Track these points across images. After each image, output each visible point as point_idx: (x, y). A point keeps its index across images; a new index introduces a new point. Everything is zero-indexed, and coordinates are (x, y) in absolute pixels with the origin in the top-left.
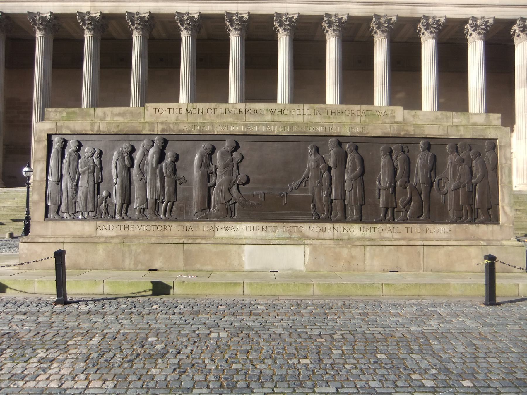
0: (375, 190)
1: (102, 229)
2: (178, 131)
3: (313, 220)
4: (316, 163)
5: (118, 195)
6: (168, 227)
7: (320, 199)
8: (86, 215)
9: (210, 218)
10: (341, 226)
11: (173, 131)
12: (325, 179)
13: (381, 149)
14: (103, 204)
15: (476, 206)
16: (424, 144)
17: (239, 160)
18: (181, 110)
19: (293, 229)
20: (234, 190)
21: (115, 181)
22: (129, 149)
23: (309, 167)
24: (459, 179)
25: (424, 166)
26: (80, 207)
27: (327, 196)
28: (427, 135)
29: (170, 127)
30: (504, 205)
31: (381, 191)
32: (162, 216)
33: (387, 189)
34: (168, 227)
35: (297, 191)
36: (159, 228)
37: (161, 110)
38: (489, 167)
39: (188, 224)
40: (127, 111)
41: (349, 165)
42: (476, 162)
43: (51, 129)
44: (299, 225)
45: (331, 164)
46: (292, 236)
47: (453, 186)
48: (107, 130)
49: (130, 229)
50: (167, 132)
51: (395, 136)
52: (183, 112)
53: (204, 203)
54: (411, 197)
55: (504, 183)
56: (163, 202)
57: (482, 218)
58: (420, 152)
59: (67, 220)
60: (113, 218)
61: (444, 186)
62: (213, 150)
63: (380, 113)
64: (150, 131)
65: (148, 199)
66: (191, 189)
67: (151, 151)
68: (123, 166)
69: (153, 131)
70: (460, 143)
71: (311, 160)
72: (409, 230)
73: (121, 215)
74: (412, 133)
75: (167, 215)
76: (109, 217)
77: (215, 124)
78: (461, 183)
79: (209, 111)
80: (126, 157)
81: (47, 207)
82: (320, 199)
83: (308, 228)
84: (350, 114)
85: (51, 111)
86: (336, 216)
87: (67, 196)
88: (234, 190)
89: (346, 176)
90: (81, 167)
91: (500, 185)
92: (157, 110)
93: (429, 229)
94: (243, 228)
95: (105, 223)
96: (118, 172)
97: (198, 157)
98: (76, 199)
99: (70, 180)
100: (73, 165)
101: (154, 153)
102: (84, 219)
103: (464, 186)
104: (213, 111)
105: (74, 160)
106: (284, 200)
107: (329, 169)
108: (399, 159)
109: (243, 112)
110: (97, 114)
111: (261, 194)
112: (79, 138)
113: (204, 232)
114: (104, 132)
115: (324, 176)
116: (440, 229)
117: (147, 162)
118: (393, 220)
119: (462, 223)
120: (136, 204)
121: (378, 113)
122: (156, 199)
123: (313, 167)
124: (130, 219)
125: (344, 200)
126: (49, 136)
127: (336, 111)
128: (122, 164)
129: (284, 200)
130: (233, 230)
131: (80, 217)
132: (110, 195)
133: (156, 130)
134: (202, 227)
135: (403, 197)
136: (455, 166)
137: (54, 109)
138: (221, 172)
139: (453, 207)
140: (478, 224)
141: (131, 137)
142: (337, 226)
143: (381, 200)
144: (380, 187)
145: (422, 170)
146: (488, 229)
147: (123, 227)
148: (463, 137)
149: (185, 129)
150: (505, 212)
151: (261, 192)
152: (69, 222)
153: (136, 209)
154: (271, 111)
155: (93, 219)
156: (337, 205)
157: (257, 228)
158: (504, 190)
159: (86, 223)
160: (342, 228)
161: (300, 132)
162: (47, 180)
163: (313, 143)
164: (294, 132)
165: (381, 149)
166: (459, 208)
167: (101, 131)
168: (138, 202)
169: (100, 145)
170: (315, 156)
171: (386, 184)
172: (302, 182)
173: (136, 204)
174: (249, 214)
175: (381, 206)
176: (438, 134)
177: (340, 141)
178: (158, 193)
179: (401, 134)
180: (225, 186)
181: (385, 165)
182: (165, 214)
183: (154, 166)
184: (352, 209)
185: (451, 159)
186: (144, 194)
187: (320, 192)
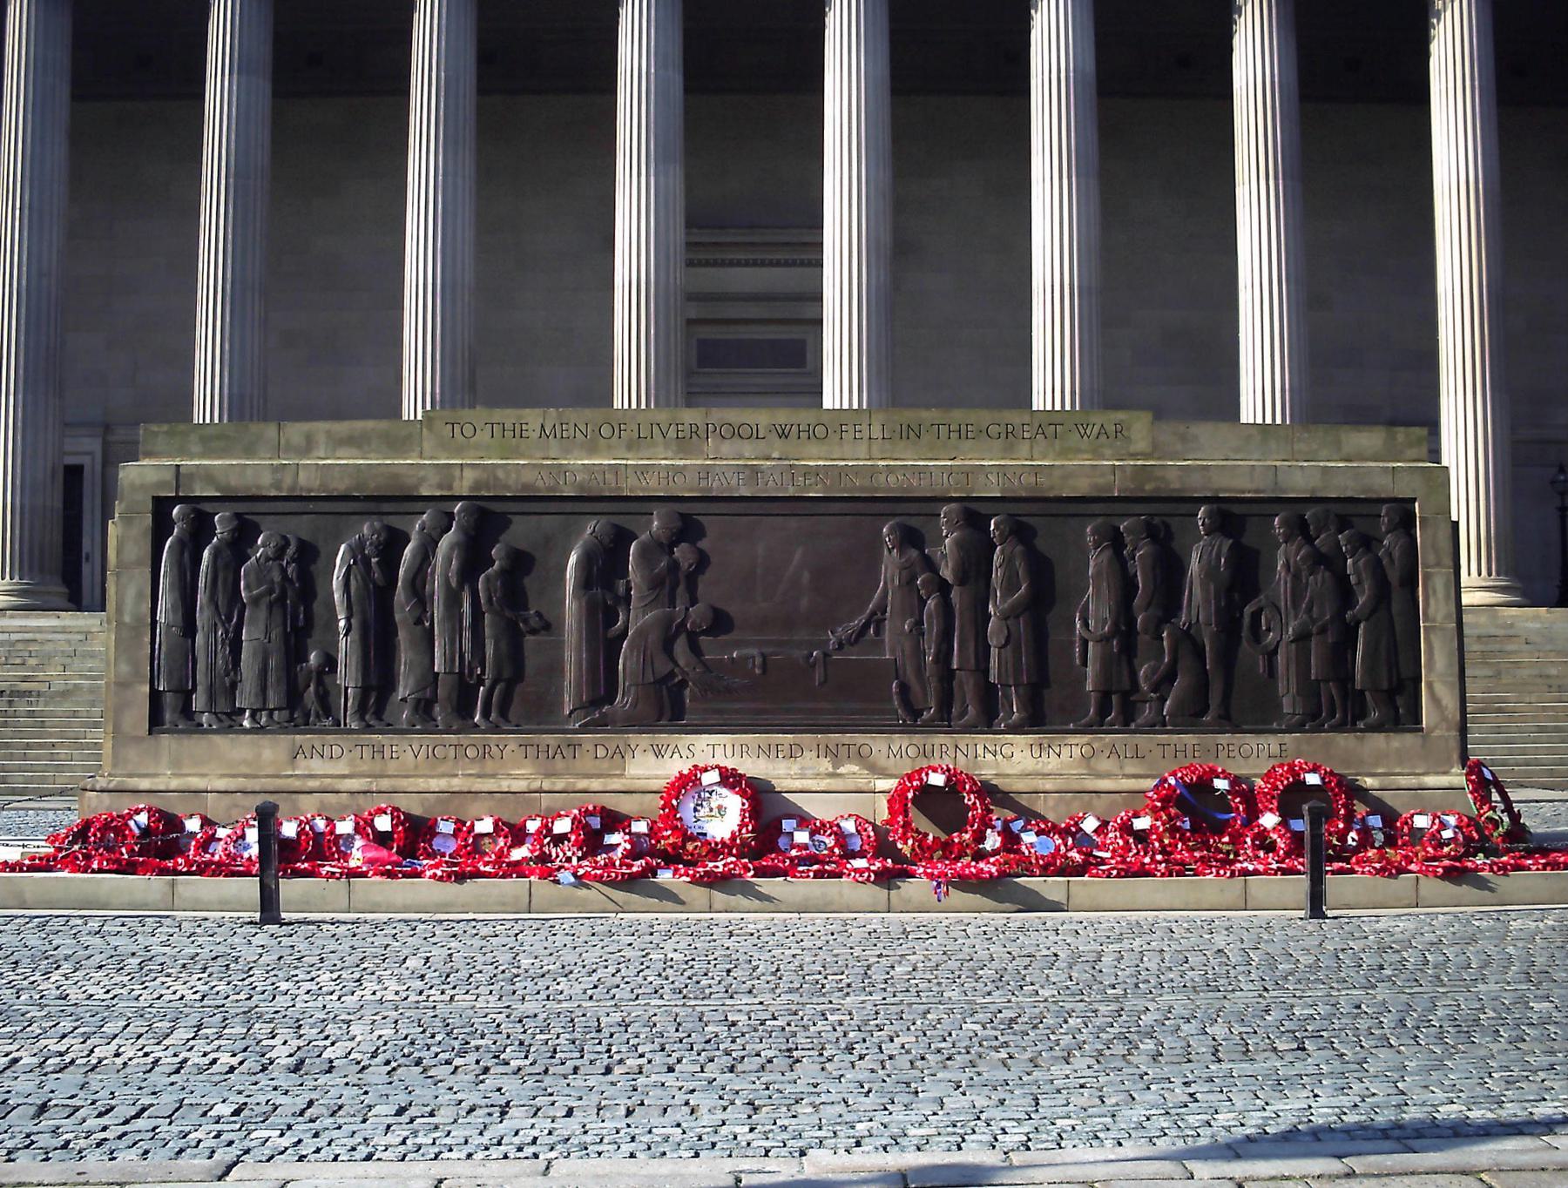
0: (1072, 643)
1: (308, 756)
2: (520, 487)
3: (900, 725)
4: (905, 573)
5: (354, 661)
6: (494, 749)
7: (920, 668)
8: (264, 719)
9: (614, 723)
10: (976, 741)
11: (507, 487)
12: (930, 617)
13: (1088, 530)
14: (312, 688)
15: (1358, 686)
16: (1209, 514)
17: (690, 566)
18: (524, 427)
19: (843, 751)
20: (681, 646)
21: (342, 624)
22: (381, 539)
23: (885, 583)
24: (1309, 610)
25: (1210, 572)
26: (245, 697)
27: (936, 660)
28: (1218, 490)
29: (496, 478)
30: (1433, 678)
31: (1091, 644)
32: (477, 718)
33: (1104, 640)
34: (494, 749)
35: (856, 648)
36: (471, 752)
37: (468, 430)
38: (1394, 576)
39: (551, 739)
40: (373, 429)
41: (997, 575)
42: (1354, 563)
43: (162, 484)
44: (859, 738)
45: (947, 573)
46: (839, 771)
47: (1290, 630)
48: (320, 485)
49: (387, 754)
50: (489, 490)
51: (1128, 494)
52: (530, 433)
53: (593, 682)
54: (1174, 661)
55: (1434, 620)
56: (481, 682)
57: (1374, 715)
58: (1200, 538)
59: (210, 731)
60: (338, 727)
61: (1269, 630)
62: (622, 538)
63: (1088, 432)
64: (440, 487)
65: (438, 674)
66: (559, 646)
67: (445, 542)
68: (366, 585)
69: (450, 488)
70: (1313, 510)
71: (890, 564)
72: (1169, 750)
73: (362, 718)
74: (1176, 485)
75: (493, 716)
76: (328, 722)
77: (623, 468)
78: (1314, 621)
79: (605, 431)
80: (374, 560)
81: (155, 697)
82: (920, 668)
83: (885, 749)
84: (1003, 436)
85: (158, 432)
86: (964, 713)
87: (211, 667)
88: (681, 646)
89: (991, 608)
90: (247, 587)
91: (1422, 625)
92: (457, 429)
93: (1226, 747)
94: (705, 748)
95: (315, 739)
96: (353, 599)
97: (578, 558)
98: (236, 674)
99: (219, 625)
100: (225, 580)
101: (452, 548)
102: (258, 730)
103: (1323, 631)
104: (617, 431)
105: (226, 566)
106: (818, 676)
107: (943, 588)
108: (1141, 556)
109: (702, 433)
110: (288, 441)
111: (753, 657)
112: (241, 508)
113: (598, 761)
114: (312, 491)
115: (929, 608)
116: (1255, 747)
117: (433, 572)
118: (1127, 721)
119: (1319, 729)
120: (404, 689)
121: (1083, 432)
122: (461, 673)
123: (897, 582)
124: (390, 729)
125: (986, 671)
126: (157, 501)
127: (963, 428)
128: (363, 578)
129: (818, 676)
130: (676, 755)
131: (246, 724)
132: (330, 662)
133: (456, 484)
134: (592, 748)
135: (1152, 663)
136: (1296, 577)
137: (165, 427)
138: (642, 598)
139: (1293, 689)
140: (1361, 731)
141: (386, 507)
142: (964, 740)
143: (1089, 669)
144: (1085, 634)
145: (1204, 584)
146: (1387, 743)
147: (367, 752)
148: (1320, 495)
149: (540, 483)
150: (1435, 699)
151: (754, 651)
152: (217, 739)
153: (404, 700)
154: (780, 431)
155: (284, 730)
156: (966, 685)
157: (745, 748)
158: (1432, 636)
159: (265, 741)
160: (980, 750)
161: (862, 489)
162: (154, 623)
163: (897, 519)
164: (844, 490)
165: (1088, 530)
166: (1309, 690)
167: (301, 489)
168: (411, 682)
169: (300, 528)
170: (901, 553)
171: (1103, 628)
172: (866, 627)
173: (405, 688)
174: (719, 712)
175: (1089, 687)
176: (1249, 486)
177: (973, 514)
178: (468, 657)
179: (1143, 490)
180: (654, 638)
181: (1098, 574)
182: (486, 714)
183: (454, 584)
184: (1007, 697)
185: (1284, 558)
186: (427, 661)
187: (919, 653)
